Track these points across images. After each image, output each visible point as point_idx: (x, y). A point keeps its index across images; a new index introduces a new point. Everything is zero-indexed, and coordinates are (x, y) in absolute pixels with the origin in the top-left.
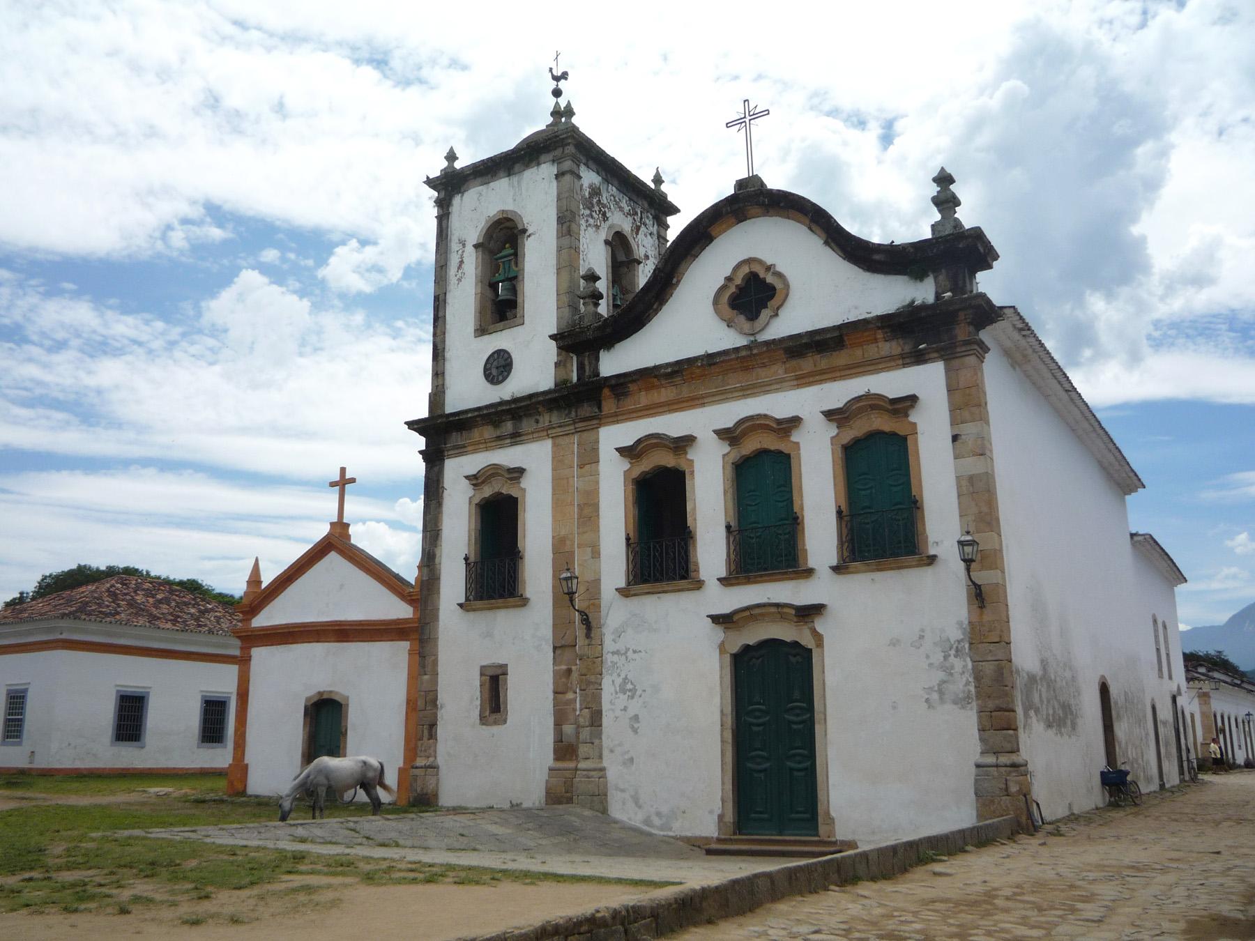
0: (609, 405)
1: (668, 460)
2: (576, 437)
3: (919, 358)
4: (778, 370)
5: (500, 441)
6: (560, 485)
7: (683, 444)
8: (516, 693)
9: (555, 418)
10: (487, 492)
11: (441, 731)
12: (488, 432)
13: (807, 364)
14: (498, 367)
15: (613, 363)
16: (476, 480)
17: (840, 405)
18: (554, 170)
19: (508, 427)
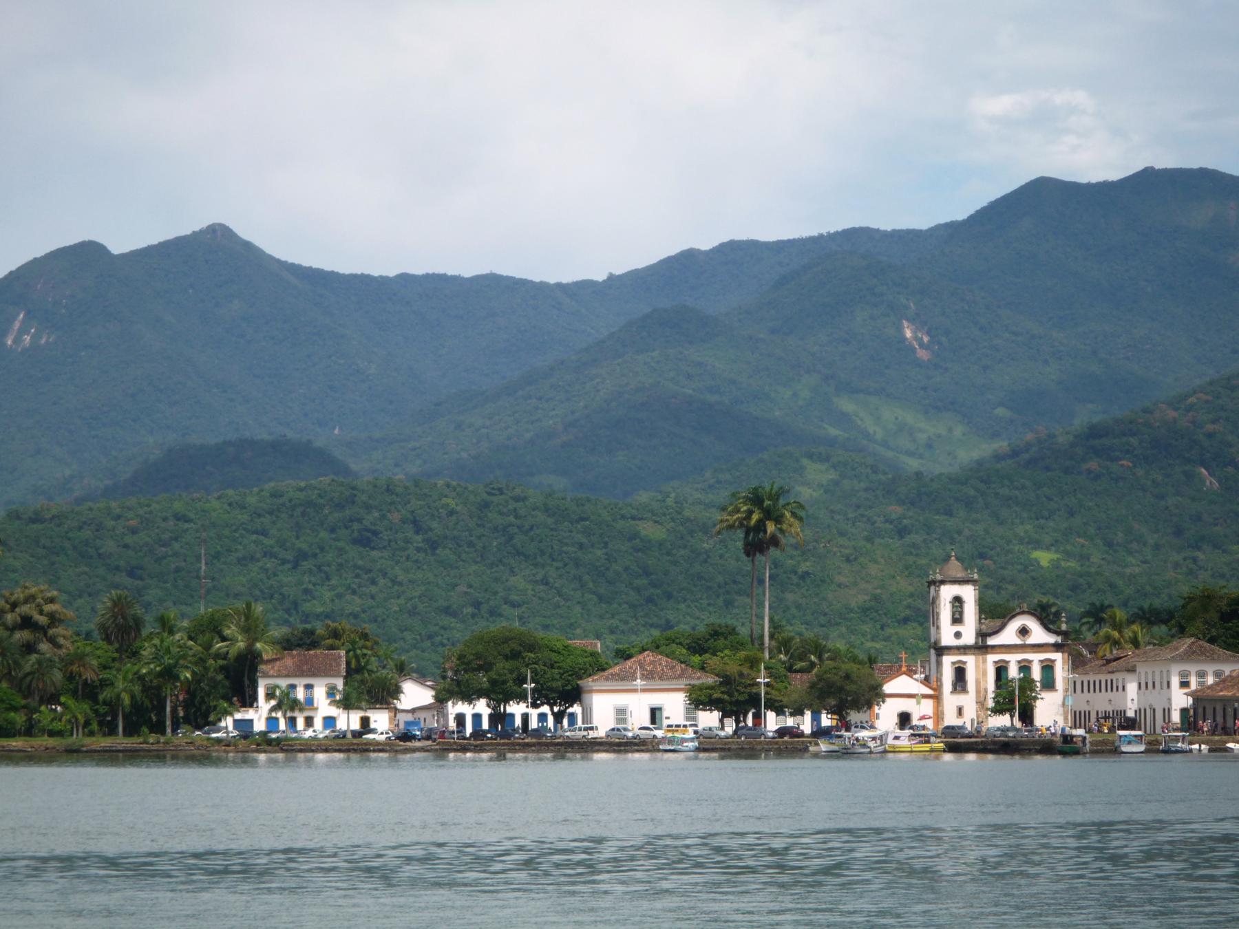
0: (989, 650)
1: (1004, 665)
2: (981, 657)
3: (1057, 652)
4: (1029, 650)
5: (960, 654)
6: (977, 667)
7: (1008, 662)
8: (965, 711)
9: (976, 652)
10: (957, 666)
11: (945, 720)
12: (956, 652)
13: (1035, 649)
14: (958, 635)
15: (991, 641)
16: (953, 663)
17: (1042, 659)
18: (973, 588)
19: (962, 650)
